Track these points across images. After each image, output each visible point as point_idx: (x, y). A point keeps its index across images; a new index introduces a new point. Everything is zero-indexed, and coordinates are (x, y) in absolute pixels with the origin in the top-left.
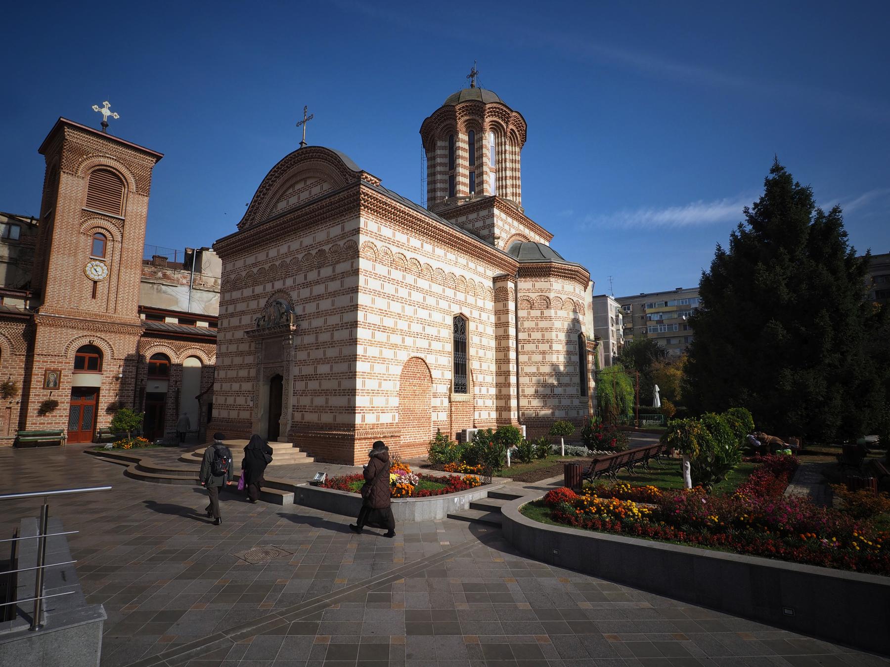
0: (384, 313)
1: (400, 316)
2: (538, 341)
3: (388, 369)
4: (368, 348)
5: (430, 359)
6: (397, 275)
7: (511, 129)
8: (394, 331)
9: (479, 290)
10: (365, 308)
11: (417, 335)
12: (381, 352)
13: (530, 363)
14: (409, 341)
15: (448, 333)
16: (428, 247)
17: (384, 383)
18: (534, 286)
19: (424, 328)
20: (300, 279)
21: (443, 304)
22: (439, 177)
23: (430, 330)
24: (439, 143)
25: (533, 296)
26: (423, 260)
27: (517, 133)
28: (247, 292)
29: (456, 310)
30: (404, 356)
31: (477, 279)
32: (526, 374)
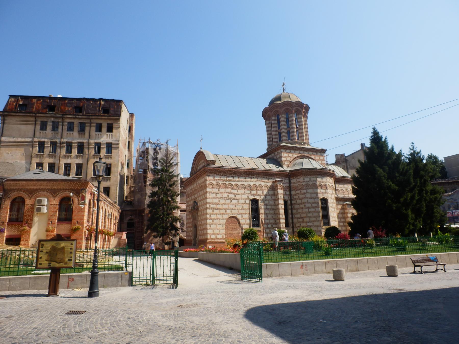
0: (217, 204)
1: (224, 204)
2: (300, 204)
3: (220, 221)
4: (211, 215)
5: (239, 217)
6: (222, 190)
7: (297, 109)
8: (221, 209)
9: (264, 188)
10: (209, 203)
11: (232, 209)
12: (216, 216)
13: (297, 214)
14: (228, 211)
15: (247, 206)
16: (236, 179)
17: (218, 226)
18: (297, 180)
19: (235, 206)
20: (199, 195)
21: (245, 196)
22: (273, 133)
23: (237, 207)
24: (273, 118)
25: (297, 185)
26: (233, 183)
27: (300, 109)
28: (190, 198)
29: (252, 197)
30: (226, 216)
31: (263, 184)
32: (297, 218)
